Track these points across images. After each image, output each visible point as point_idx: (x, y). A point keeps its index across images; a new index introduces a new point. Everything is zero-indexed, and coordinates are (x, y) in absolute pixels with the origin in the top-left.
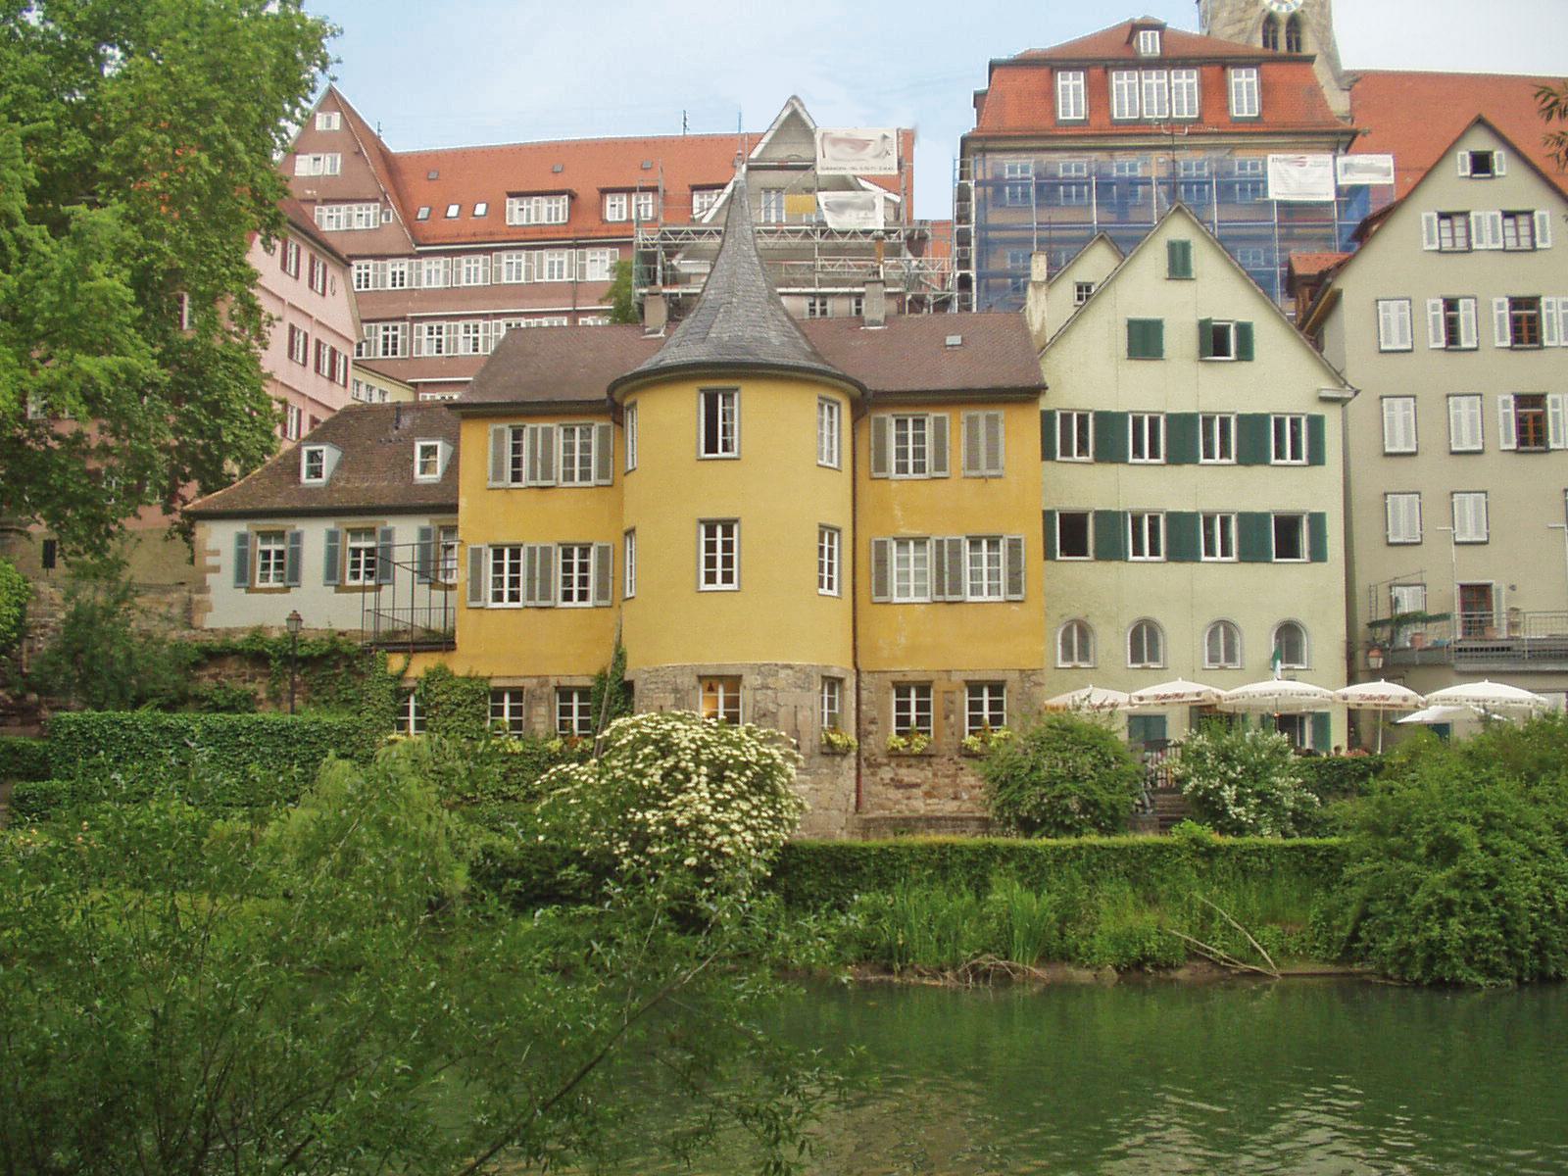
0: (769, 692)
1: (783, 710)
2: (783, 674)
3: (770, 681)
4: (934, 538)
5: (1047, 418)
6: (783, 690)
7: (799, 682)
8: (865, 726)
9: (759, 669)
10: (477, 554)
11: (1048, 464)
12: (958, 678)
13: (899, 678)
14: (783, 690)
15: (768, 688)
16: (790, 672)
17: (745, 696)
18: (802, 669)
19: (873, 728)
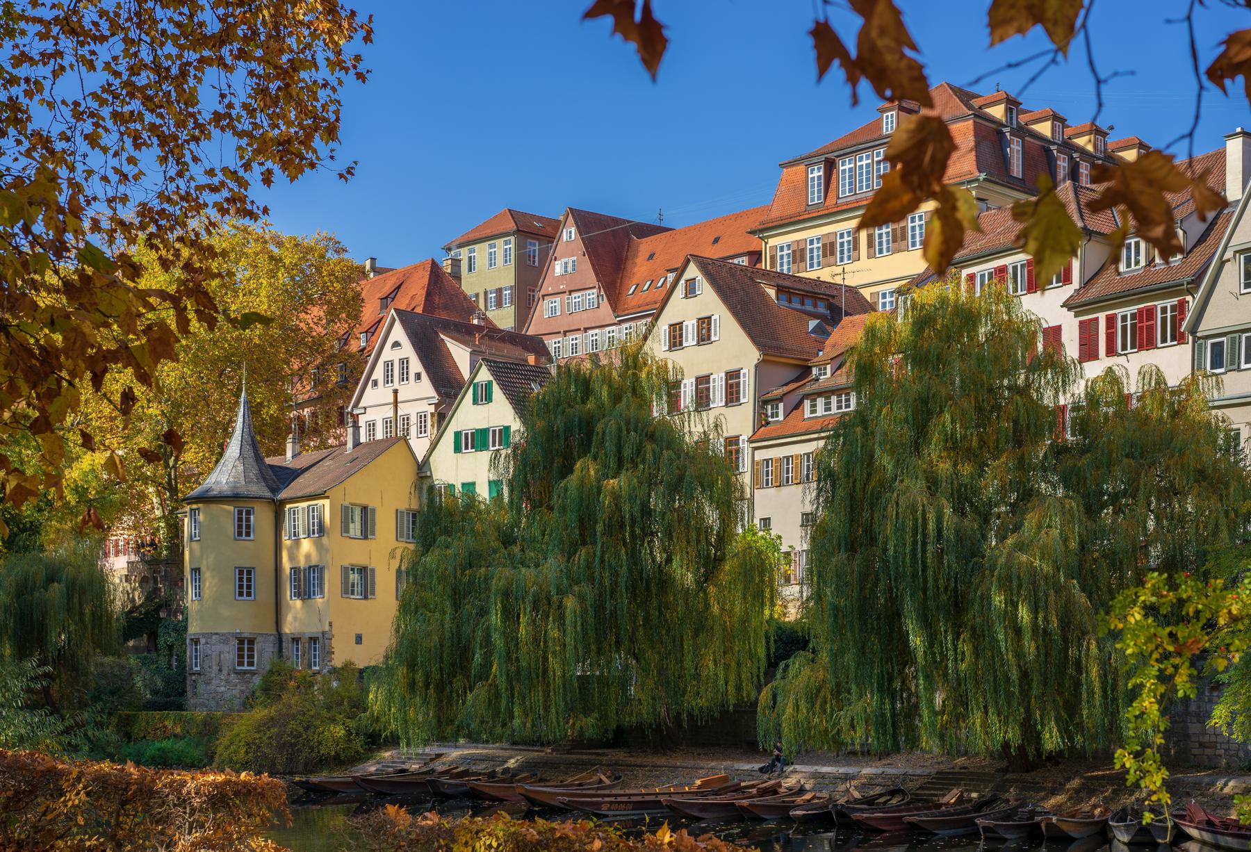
9: (203, 634)
18: (223, 635)
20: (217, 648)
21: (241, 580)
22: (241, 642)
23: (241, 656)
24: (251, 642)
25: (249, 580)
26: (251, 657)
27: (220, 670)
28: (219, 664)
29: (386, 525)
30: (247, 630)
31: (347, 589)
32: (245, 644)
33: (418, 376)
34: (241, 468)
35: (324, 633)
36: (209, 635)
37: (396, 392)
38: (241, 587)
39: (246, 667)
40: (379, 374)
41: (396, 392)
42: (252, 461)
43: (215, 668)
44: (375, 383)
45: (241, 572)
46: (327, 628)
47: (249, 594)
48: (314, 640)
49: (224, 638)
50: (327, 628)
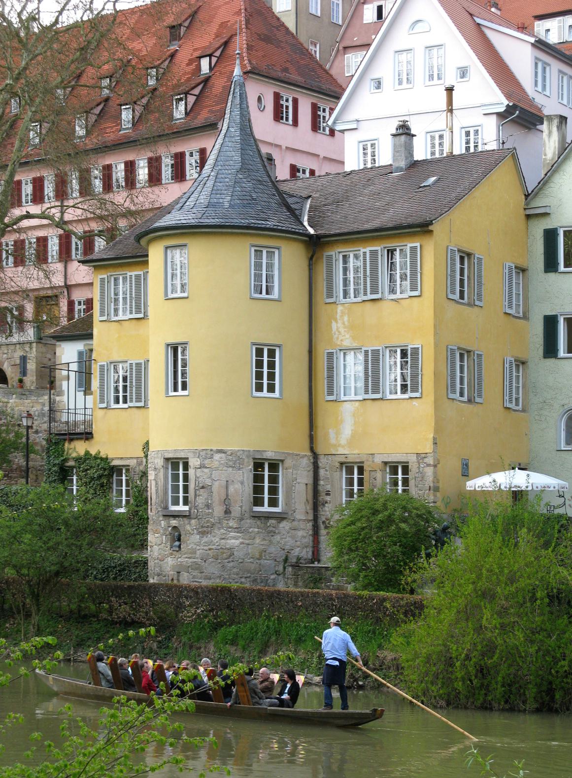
0: (206, 470)
1: (216, 484)
2: (217, 457)
3: (207, 462)
4: (364, 349)
6: (217, 469)
7: (231, 463)
8: (323, 497)
9: (197, 453)
10: (102, 367)
12: (378, 460)
13: (343, 460)
14: (217, 469)
15: (206, 468)
16: (223, 455)
17: (191, 472)
19: (328, 498)
22: (258, 465)
23: (258, 490)
24: (274, 466)
26: (273, 491)
28: (227, 502)
31: (448, 385)
32: (264, 471)
33: (463, 73)
36: (209, 454)
37: (450, 90)
38: (259, 376)
39: (266, 508)
41: (450, 90)
44: (378, 84)
47: (271, 389)
49: (234, 460)
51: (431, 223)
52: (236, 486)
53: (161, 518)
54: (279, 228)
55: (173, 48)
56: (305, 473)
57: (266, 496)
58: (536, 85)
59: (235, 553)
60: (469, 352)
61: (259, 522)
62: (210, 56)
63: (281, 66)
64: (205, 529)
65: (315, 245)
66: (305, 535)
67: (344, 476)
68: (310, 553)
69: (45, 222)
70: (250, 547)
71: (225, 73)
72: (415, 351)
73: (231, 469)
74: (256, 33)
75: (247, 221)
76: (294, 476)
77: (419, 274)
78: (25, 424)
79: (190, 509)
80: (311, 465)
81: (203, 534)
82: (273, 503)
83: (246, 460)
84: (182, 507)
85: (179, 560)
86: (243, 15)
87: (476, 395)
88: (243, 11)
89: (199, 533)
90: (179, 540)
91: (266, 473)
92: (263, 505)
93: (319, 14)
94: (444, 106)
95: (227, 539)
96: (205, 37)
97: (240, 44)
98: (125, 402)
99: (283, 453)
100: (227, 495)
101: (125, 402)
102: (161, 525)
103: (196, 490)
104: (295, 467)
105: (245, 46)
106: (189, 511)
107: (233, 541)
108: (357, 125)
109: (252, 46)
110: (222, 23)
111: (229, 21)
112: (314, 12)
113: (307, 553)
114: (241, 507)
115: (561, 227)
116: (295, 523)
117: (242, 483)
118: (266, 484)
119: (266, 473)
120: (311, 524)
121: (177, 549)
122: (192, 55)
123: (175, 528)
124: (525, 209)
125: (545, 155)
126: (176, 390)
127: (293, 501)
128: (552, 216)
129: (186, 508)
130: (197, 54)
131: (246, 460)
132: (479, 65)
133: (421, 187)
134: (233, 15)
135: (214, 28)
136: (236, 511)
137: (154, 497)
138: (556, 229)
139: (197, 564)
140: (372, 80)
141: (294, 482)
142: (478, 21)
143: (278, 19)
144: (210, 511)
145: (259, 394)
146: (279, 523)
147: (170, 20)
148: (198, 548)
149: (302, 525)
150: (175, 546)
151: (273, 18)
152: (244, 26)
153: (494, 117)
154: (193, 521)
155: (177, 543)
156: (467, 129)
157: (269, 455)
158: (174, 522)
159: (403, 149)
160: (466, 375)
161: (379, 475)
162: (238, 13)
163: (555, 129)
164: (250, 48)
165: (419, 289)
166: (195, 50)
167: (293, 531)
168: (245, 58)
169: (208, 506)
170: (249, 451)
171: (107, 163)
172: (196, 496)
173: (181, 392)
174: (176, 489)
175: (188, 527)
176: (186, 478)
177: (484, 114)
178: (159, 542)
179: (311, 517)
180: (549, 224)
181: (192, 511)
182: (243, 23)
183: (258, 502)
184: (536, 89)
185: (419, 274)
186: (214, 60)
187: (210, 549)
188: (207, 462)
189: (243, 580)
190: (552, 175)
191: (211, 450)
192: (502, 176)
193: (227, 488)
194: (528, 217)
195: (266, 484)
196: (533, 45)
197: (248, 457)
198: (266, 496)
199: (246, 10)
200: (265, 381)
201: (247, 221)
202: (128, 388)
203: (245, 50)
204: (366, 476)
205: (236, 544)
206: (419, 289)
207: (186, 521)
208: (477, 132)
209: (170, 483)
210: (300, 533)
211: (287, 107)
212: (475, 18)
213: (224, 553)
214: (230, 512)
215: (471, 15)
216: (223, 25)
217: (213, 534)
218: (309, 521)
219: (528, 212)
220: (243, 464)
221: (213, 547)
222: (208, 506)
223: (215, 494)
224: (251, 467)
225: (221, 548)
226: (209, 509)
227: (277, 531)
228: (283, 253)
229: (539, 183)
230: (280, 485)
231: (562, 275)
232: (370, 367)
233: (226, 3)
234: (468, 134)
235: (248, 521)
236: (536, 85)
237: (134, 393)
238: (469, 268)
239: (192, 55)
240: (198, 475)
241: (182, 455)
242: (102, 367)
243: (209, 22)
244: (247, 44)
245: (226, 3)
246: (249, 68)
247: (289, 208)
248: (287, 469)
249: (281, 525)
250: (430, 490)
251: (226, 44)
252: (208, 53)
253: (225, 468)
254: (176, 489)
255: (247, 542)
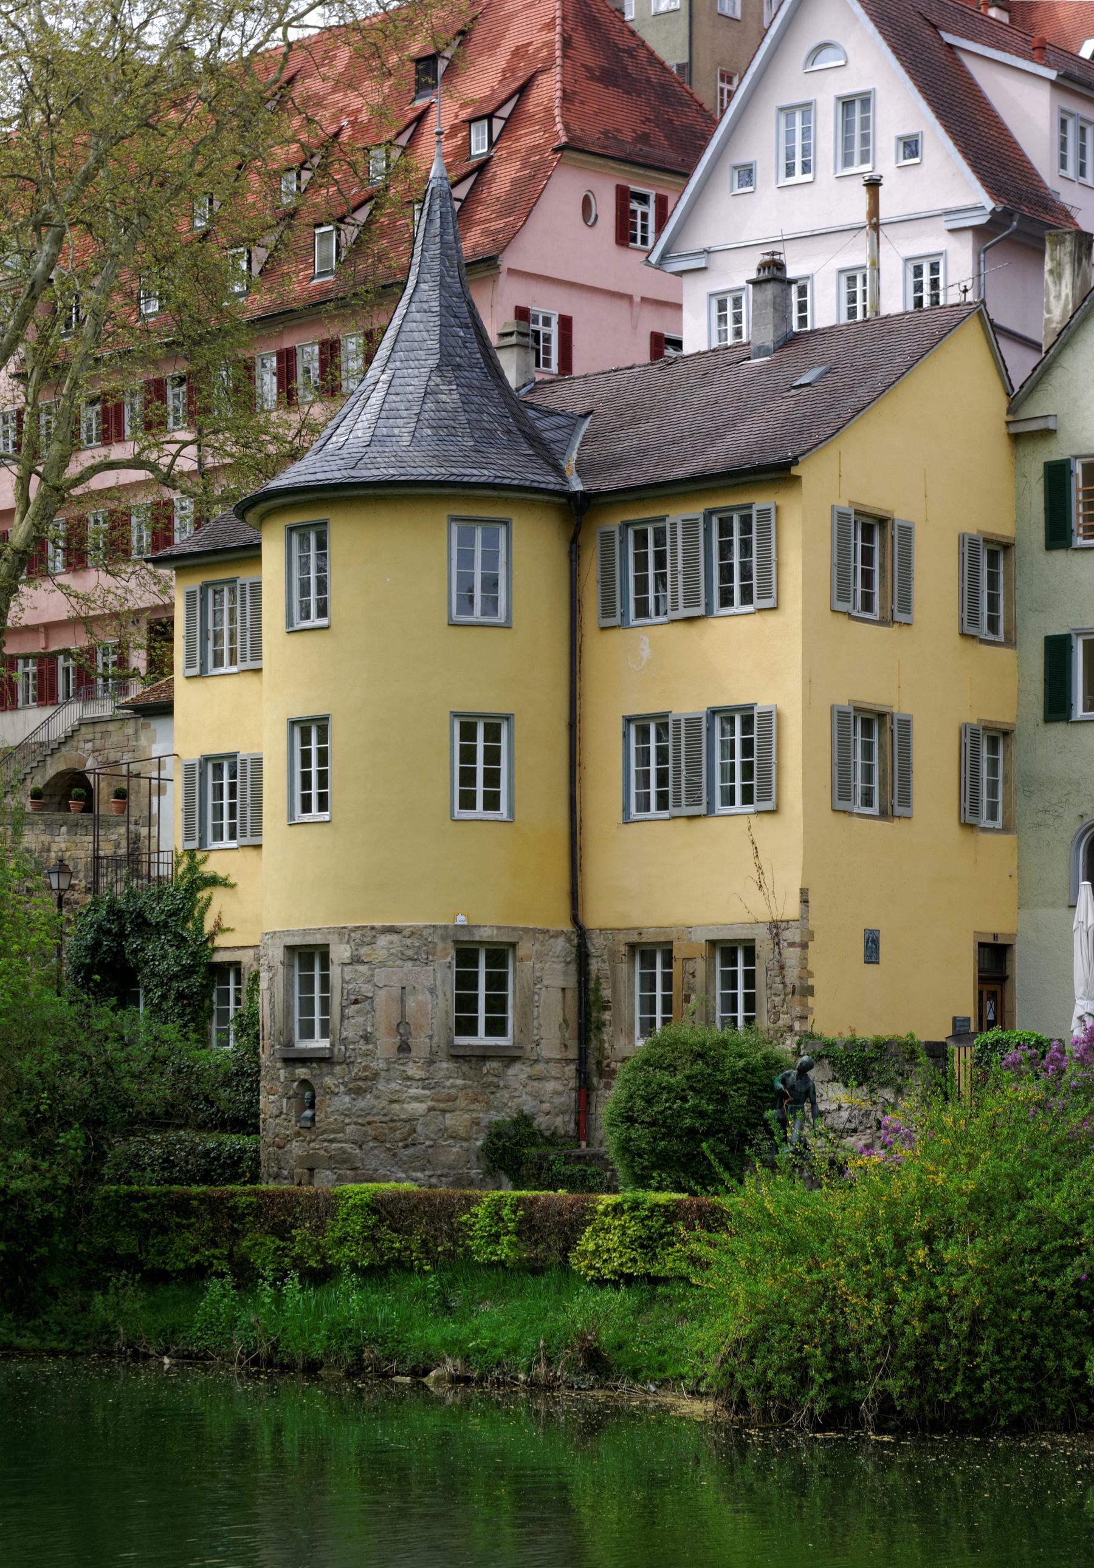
0: (362, 968)
2: (383, 940)
5: (1057, 475)
6: (382, 964)
7: (410, 953)
9: (344, 933)
10: (189, 768)
11: (1060, 556)
12: (701, 937)
13: (634, 938)
14: (382, 964)
15: (363, 962)
17: (335, 971)
19: (607, 1016)
20: (391, 977)
21: (468, 754)
22: (466, 955)
23: (466, 1003)
24: (499, 955)
25: (493, 756)
26: (497, 1004)
27: (404, 1048)
28: (402, 1026)
29: (936, 578)
30: (486, 916)
32: (480, 965)
33: (911, 146)
34: (450, 396)
35: (776, 927)
36: (369, 935)
37: (873, 185)
38: (468, 776)
39: (481, 1039)
40: (761, 144)
41: (873, 185)
42: (474, 376)
43: (386, 1044)
45: (468, 732)
46: (791, 909)
47: (492, 802)
48: (730, 950)
49: (417, 945)
50: (791, 909)
51: (795, 461)
52: (420, 997)
53: (279, 1065)
54: (507, 481)
55: (421, 103)
56: (560, 967)
57: (482, 1015)
58: (1063, 165)
59: (419, 1128)
60: (881, 716)
61: (465, 1068)
62: (490, 117)
63: (634, 131)
64: (361, 1083)
65: (576, 512)
66: (561, 1088)
67: (638, 971)
68: (573, 1125)
69: (141, 475)
70: (448, 1115)
71: (517, 152)
72: (766, 715)
73: (410, 963)
74: (583, 66)
75: (443, 470)
76: (538, 974)
77: (774, 565)
78: (55, 886)
79: (332, 1044)
80: (574, 950)
81: (358, 1092)
82: (496, 1027)
83: (440, 945)
84: (319, 1043)
85: (312, 1145)
86: (558, 29)
87: (896, 801)
88: (558, 21)
89: (350, 1091)
90: (312, 1106)
91: (482, 970)
92: (474, 1032)
93: (738, 15)
94: (860, 216)
95: (403, 1102)
96: (484, 79)
97: (549, 89)
98: (232, 837)
99: (515, 929)
100: (403, 1015)
101: (232, 837)
102: (278, 1078)
103: (343, 1008)
104: (541, 957)
105: (559, 94)
106: (331, 1049)
107: (415, 1105)
108: (708, 261)
109: (574, 93)
110: (518, 48)
111: (530, 44)
112: (727, 11)
113: (564, 1124)
114: (431, 1037)
115: (1076, 457)
116: (540, 1067)
117: (432, 991)
118: (482, 992)
119: (482, 970)
120: (573, 1067)
121: (309, 1124)
122: (457, 116)
123: (304, 1083)
124: (1008, 423)
125: (1049, 311)
126: (306, 808)
127: (536, 1023)
128: (1061, 435)
129: (326, 1043)
130: (464, 114)
131: (440, 945)
132: (940, 131)
133: (794, 388)
134: (540, 30)
135: (501, 59)
136: (421, 1044)
137: (267, 1023)
138: (1069, 460)
139: (345, 1152)
140: (735, 168)
141: (541, 984)
142: (949, 38)
143: (633, 33)
144: (370, 1047)
145: (467, 814)
146: (507, 1066)
147: (417, 46)
148: (347, 1121)
149: (554, 1070)
150: (306, 1118)
151: (621, 31)
152: (558, 53)
153: (968, 238)
154: (338, 1069)
155: (308, 1113)
156: (917, 262)
157: (485, 935)
158: (302, 1072)
159: (770, 310)
160: (876, 761)
161: (700, 966)
162: (550, 26)
163: (1067, 260)
164: (567, 97)
165: (774, 594)
166: (463, 106)
167: (535, 1083)
168: (558, 119)
169: (367, 1038)
170: (446, 927)
171: (287, 344)
172: (343, 1017)
173: (315, 814)
174: (307, 1007)
175: (328, 1081)
176: (325, 981)
177: (951, 231)
178: (275, 1112)
179: (573, 1053)
180: (1057, 452)
181: (336, 1050)
182: (558, 45)
183: (466, 1027)
184: (1063, 172)
185: (774, 565)
186: (498, 125)
187: (369, 1123)
188: (363, 951)
189: (434, 1180)
190: (1059, 353)
191: (373, 928)
192: (964, 360)
193: (402, 1001)
194: (1016, 439)
195: (482, 992)
196: (1053, 83)
197: (444, 939)
198: (482, 1015)
199: (564, 19)
200: (480, 788)
201: (443, 470)
202: (238, 809)
203: (557, 102)
204: (676, 969)
205: (421, 1111)
206: (774, 594)
207: (325, 1069)
208: (934, 269)
209: (297, 994)
210: (551, 1086)
211: (645, 216)
212: (943, 34)
213: (393, 1130)
214: (409, 1050)
215: (935, 27)
216: (519, 52)
217: (375, 1092)
218: (568, 1061)
219: (1015, 429)
220: (434, 954)
221: (376, 1119)
222: (367, 1038)
223: (380, 1015)
224: (451, 957)
225: (392, 1121)
226: (367, 1043)
227: (502, 1084)
228: (515, 531)
229: (1035, 369)
230: (510, 992)
231: (1079, 555)
232: (683, 753)
233: (530, 6)
234: (918, 271)
235: (445, 1065)
236: (1063, 165)
237: (249, 818)
238: (883, 547)
239: (457, 116)
240: (347, 978)
241: (318, 940)
242: (189, 768)
243: (493, 47)
244: (564, 90)
245: (530, 6)
246: (564, 139)
247: (534, 439)
248: (522, 960)
249: (511, 1071)
250: (793, 993)
251: (523, 90)
252: (486, 111)
253: (399, 963)
254: (307, 1007)
255: (442, 1106)
